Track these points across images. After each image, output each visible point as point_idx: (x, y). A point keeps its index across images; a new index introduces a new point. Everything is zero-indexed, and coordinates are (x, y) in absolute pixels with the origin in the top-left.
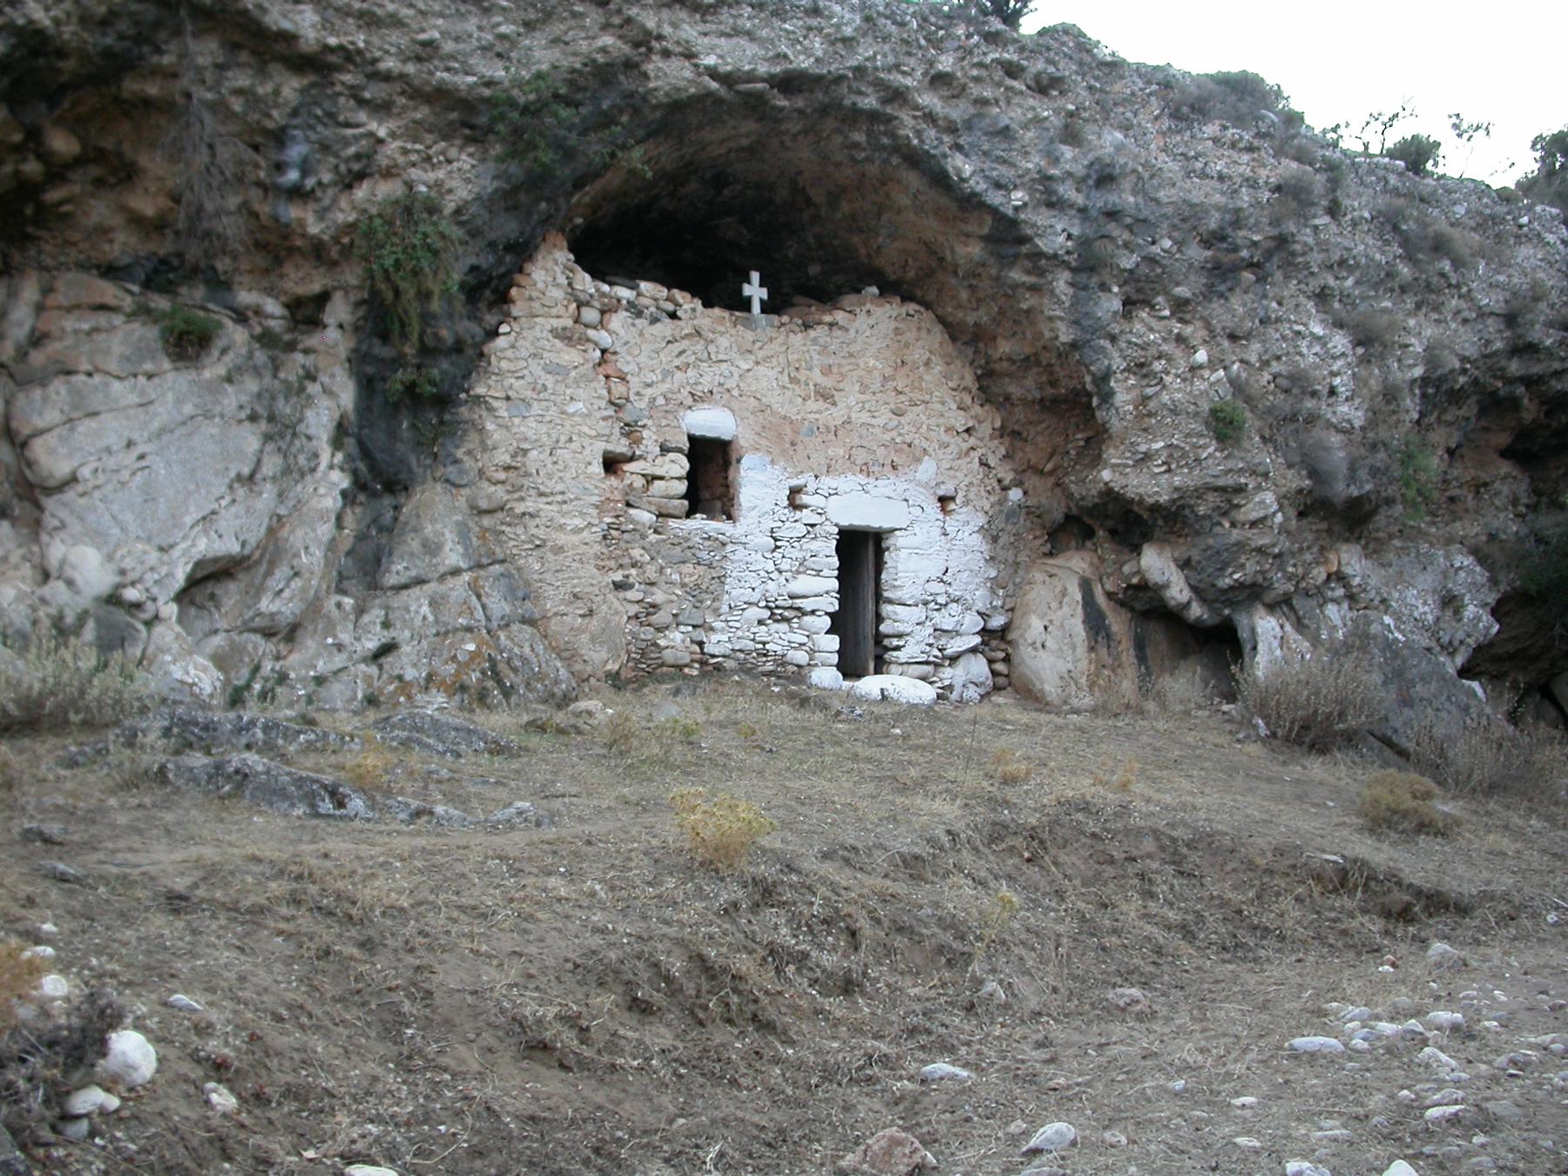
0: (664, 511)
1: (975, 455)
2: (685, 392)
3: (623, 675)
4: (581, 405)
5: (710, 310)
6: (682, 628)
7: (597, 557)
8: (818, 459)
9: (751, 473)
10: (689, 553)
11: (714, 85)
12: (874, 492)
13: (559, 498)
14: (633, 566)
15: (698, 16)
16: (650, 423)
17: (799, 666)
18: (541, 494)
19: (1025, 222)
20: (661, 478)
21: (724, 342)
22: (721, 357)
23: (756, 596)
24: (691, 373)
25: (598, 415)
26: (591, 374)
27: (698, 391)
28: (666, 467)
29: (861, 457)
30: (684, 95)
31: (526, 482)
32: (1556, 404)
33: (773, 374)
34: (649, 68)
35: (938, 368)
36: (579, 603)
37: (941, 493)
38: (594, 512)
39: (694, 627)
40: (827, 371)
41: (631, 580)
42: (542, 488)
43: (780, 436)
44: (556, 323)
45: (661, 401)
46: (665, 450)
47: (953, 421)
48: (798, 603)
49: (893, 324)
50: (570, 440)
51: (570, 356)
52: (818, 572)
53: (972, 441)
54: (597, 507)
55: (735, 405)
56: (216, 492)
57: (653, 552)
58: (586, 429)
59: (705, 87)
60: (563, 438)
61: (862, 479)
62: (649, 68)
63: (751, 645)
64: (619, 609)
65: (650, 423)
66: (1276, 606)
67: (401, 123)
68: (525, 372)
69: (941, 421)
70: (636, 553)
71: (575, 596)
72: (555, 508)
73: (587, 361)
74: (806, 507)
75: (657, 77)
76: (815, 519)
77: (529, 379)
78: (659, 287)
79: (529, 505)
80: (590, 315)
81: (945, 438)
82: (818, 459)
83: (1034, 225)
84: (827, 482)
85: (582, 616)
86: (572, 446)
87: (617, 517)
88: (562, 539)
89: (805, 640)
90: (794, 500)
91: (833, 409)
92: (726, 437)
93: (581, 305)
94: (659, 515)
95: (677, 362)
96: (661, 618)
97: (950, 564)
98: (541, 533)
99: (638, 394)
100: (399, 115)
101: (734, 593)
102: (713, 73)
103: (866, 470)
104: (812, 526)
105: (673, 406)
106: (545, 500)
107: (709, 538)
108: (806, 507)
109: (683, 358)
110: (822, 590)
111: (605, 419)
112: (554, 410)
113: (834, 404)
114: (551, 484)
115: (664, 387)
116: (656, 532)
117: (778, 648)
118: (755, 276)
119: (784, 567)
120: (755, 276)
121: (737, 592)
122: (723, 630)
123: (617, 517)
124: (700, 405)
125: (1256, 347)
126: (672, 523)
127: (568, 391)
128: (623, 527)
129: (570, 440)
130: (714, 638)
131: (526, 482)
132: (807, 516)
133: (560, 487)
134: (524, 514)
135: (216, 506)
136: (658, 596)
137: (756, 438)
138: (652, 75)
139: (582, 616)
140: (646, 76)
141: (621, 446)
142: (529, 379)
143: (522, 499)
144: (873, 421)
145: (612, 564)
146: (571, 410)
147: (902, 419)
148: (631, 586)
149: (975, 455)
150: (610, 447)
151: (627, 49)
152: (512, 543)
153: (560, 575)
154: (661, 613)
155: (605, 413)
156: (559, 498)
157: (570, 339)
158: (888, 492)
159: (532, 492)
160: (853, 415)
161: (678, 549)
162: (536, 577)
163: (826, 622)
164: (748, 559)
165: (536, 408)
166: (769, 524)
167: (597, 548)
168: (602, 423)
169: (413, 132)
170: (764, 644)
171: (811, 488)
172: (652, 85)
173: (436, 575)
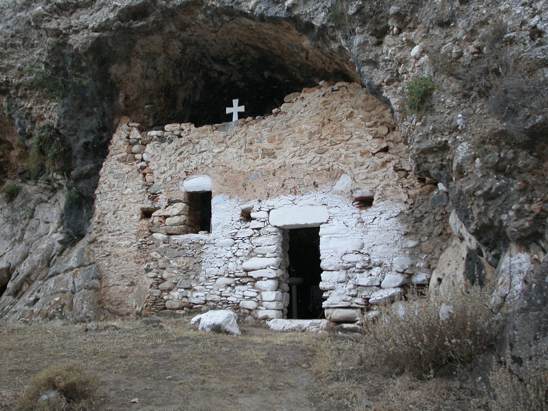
0: (170, 232)
1: (391, 165)
2: (182, 172)
3: (143, 313)
4: (129, 189)
5: (200, 128)
6: (179, 290)
7: (135, 258)
8: (261, 190)
9: (217, 206)
10: (181, 251)
11: (96, 34)
12: (301, 203)
13: (118, 233)
14: (152, 260)
15: (89, 8)
16: (163, 191)
17: (249, 310)
18: (109, 232)
19: (299, 15)
20: (169, 216)
21: (204, 142)
22: (202, 150)
23: (221, 271)
24: (186, 161)
25: (138, 192)
26: (135, 175)
27: (189, 170)
28: (170, 211)
29: (291, 184)
30: (89, 44)
31: (103, 228)
32: (269, 1)
33: (235, 150)
34: (70, 41)
35: (360, 115)
36: (125, 280)
37: (358, 194)
38: (134, 237)
39: (186, 289)
40: (271, 141)
41: (151, 267)
42: (109, 229)
43: (236, 183)
44: (119, 156)
45: (169, 179)
46: (170, 202)
47: (368, 148)
48: (250, 274)
49: (322, 99)
50: (124, 206)
51: (126, 168)
52: (264, 256)
53: (387, 156)
54: (135, 234)
55: (211, 172)
56: (6, 246)
57: (163, 253)
58: (132, 200)
59: (93, 37)
60: (121, 206)
61: (291, 197)
62: (70, 41)
63: (217, 298)
64: (147, 280)
65: (163, 191)
66: (414, 247)
67: (33, 99)
68: (107, 180)
69: (358, 149)
70: (153, 254)
71: (123, 276)
72: (115, 237)
73: (133, 169)
74: (254, 219)
75: (74, 44)
76: (259, 225)
77: (108, 183)
78: (173, 125)
79: (105, 238)
80: (135, 148)
81: (360, 159)
82: (261, 190)
83: (306, 14)
84: (267, 203)
85: (128, 285)
86: (125, 209)
87: (145, 238)
88: (119, 251)
89: (255, 294)
90: (247, 216)
91: (274, 161)
92: (208, 189)
93: (132, 145)
94: (169, 234)
95: (178, 158)
96: (166, 285)
97: (365, 241)
98: (108, 249)
99: (158, 178)
100: (31, 97)
101: (207, 270)
102: (95, 30)
103: (295, 191)
104: (258, 229)
105: (176, 180)
106: (111, 234)
107: (193, 243)
108: (254, 219)
109: (182, 156)
110: (264, 265)
111: (141, 193)
112: (118, 195)
113: (275, 157)
114: (113, 227)
115: (170, 172)
116: (164, 243)
117: (234, 300)
118: (235, 102)
119: (238, 254)
120: (235, 102)
121: (208, 269)
122: (201, 291)
123: (145, 238)
124: (190, 177)
125: (462, 23)
126: (173, 238)
127: (125, 184)
128: (148, 243)
129: (124, 206)
130: (195, 294)
131: (103, 228)
132: (254, 224)
133: (118, 228)
134: (102, 242)
135: (5, 251)
136: (165, 275)
137: (221, 187)
138: (73, 44)
139: (128, 285)
140: (71, 45)
141: (148, 204)
142: (108, 183)
143: (101, 235)
144: (302, 161)
145: (143, 260)
146: (126, 192)
147: (324, 156)
148: (151, 270)
149: (391, 165)
150: (143, 206)
151: (55, 40)
152: (96, 255)
153: (117, 268)
154: (166, 283)
155: (141, 191)
156: (118, 233)
157: (125, 161)
158: (311, 201)
159: (106, 232)
160: (287, 161)
161: (177, 250)
162: (106, 269)
163: (272, 283)
164: (215, 251)
165: (109, 195)
166: (228, 232)
167: (136, 253)
168: (140, 195)
169: (39, 102)
170: (227, 297)
171: (256, 207)
172: (75, 48)
173: (63, 271)
